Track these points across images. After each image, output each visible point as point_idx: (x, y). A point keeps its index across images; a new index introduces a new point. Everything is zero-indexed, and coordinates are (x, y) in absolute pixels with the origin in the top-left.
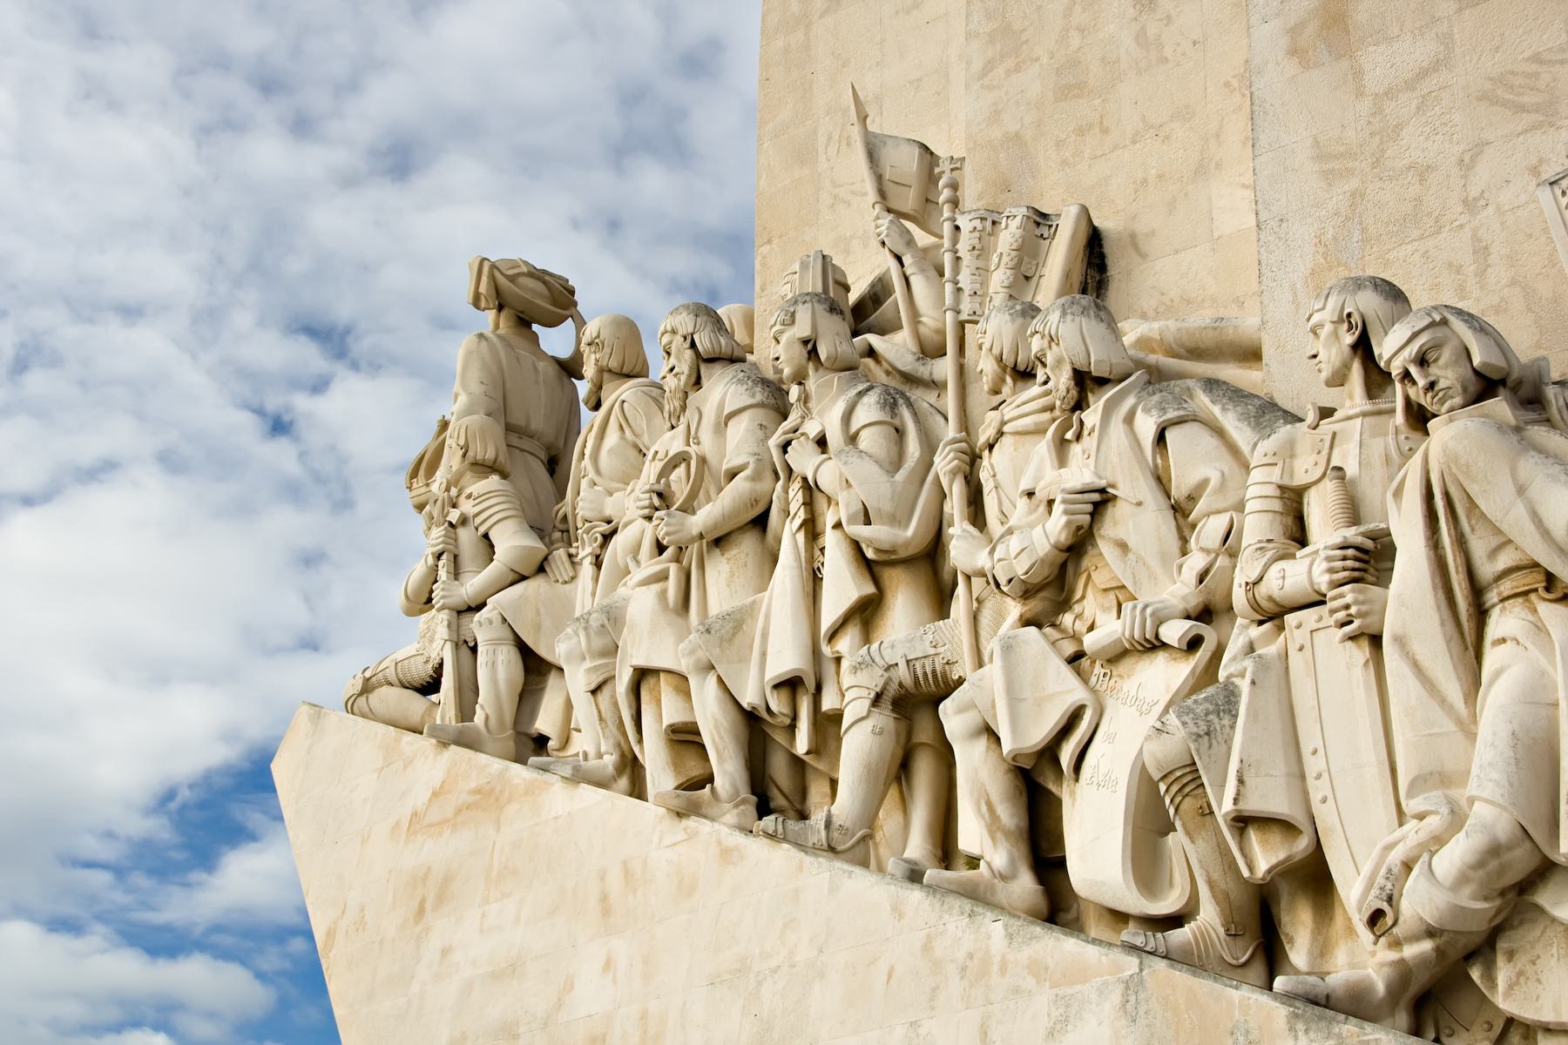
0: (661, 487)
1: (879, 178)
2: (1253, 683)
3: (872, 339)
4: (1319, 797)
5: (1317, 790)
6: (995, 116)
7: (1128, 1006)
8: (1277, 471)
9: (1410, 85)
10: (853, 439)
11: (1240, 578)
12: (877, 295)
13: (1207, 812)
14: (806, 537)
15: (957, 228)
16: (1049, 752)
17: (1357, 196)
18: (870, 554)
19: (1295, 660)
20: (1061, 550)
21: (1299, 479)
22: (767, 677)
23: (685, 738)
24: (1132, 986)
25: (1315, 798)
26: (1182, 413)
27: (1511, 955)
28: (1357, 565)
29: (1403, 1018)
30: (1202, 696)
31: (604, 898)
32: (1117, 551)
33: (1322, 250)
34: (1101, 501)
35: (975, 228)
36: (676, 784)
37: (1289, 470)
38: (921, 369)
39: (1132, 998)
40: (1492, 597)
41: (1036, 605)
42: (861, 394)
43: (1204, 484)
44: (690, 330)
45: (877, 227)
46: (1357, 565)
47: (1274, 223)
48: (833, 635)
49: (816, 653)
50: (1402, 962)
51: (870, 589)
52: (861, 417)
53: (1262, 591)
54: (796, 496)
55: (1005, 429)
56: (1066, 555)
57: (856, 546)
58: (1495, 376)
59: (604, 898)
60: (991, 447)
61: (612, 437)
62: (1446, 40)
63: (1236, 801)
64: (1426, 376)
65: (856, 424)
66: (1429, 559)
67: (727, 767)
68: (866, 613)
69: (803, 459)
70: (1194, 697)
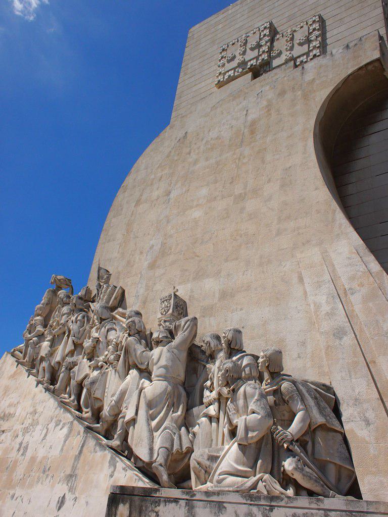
1: (99, 275)
29: (103, 433)
51: (73, 348)
52: (79, 318)
57: (73, 341)
68: (72, 353)
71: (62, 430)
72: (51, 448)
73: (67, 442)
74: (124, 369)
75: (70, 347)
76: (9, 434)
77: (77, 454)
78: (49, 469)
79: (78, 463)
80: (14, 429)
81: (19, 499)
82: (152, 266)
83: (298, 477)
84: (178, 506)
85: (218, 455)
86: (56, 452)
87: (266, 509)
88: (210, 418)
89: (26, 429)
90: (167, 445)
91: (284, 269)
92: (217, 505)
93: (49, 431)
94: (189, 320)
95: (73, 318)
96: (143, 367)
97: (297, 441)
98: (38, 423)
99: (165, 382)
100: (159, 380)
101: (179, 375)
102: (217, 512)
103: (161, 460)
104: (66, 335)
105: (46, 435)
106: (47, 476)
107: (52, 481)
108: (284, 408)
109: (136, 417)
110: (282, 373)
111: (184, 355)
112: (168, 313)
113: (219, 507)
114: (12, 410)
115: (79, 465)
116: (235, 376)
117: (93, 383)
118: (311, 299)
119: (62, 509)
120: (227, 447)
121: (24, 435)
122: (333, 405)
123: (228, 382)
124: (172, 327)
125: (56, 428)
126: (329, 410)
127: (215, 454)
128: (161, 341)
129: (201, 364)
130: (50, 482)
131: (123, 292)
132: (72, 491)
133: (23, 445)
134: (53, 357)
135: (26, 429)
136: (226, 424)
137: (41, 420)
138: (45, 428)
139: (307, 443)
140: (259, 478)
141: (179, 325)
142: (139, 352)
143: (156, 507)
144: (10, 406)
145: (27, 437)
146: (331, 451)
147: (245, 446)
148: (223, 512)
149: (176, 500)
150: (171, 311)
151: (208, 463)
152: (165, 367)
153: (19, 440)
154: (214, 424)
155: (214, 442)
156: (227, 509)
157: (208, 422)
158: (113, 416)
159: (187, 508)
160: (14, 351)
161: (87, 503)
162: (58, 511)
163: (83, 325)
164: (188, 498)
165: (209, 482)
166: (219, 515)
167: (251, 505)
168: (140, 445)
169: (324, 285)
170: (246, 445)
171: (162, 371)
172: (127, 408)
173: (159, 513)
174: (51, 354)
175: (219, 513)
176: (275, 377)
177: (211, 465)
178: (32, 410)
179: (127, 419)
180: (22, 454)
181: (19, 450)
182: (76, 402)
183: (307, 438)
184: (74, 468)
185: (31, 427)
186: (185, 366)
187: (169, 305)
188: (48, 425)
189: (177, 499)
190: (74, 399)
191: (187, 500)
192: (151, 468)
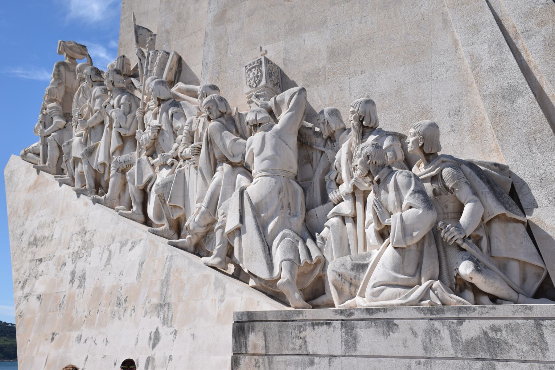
14: (109, 129)
16: (146, 186)
20: (152, 140)
29: (192, 249)
32: (162, 141)
37: (191, 127)
43: (179, 127)
47: (205, 64)
48: (113, 154)
50: (190, 238)
51: (121, 143)
52: (122, 101)
54: (107, 118)
71: (134, 250)
72: (121, 274)
73: (144, 265)
75: (115, 143)
76: (51, 262)
77: (163, 278)
78: (126, 301)
79: (167, 289)
80: (57, 254)
81: (89, 341)
83: (479, 281)
84: (332, 328)
85: (366, 262)
86: (131, 279)
87: (453, 323)
88: (343, 219)
89: (75, 254)
90: (291, 257)
91: (422, 10)
92: (385, 323)
93: (112, 254)
94: (295, 93)
95: (114, 102)
96: (237, 160)
97: (469, 238)
98: (92, 245)
100: (265, 176)
101: (291, 167)
102: (386, 331)
103: (285, 276)
104: (107, 125)
105: (109, 259)
106: (125, 309)
107: (133, 315)
108: (447, 199)
109: (241, 225)
110: (439, 154)
111: (293, 141)
112: (261, 85)
113: (388, 325)
114: (46, 232)
115: (169, 292)
116: (379, 162)
117: (166, 185)
118: (462, 52)
119: (157, 347)
120: (375, 253)
121: (74, 261)
122: (509, 189)
123: (369, 172)
124: (271, 103)
125: (124, 248)
126: (507, 196)
127: (361, 262)
128: (260, 124)
130: (131, 316)
131: (180, 59)
132: (167, 323)
133: (77, 275)
135: (75, 254)
136: (369, 224)
137: (96, 240)
138: (105, 251)
139: (481, 238)
140: (427, 286)
141: (282, 101)
143: (300, 332)
144: (40, 227)
145: (81, 265)
146: (513, 246)
147: (402, 249)
148: (394, 330)
149: (328, 322)
150: (263, 82)
151: (353, 274)
153: (69, 268)
154: (349, 225)
155: (352, 248)
156: (400, 326)
158: (204, 226)
159: (344, 330)
160: (26, 153)
161: (193, 335)
162: (152, 349)
164: (344, 318)
165: (359, 295)
166: (390, 335)
167: (431, 319)
168: (253, 259)
169: (484, 28)
170: (404, 248)
172: (225, 215)
173: (307, 339)
174: (90, 152)
175: (388, 332)
176: (431, 159)
177: (358, 276)
178: (78, 229)
179: (229, 228)
180: (78, 286)
181: (72, 281)
183: (482, 233)
184: (163, 296)
185: (83, 251)
186: (297, 154)
187: (259, 74)
188: (109, 246)
189: (328, 320)
191: (342, 320)
192: (276, 287)
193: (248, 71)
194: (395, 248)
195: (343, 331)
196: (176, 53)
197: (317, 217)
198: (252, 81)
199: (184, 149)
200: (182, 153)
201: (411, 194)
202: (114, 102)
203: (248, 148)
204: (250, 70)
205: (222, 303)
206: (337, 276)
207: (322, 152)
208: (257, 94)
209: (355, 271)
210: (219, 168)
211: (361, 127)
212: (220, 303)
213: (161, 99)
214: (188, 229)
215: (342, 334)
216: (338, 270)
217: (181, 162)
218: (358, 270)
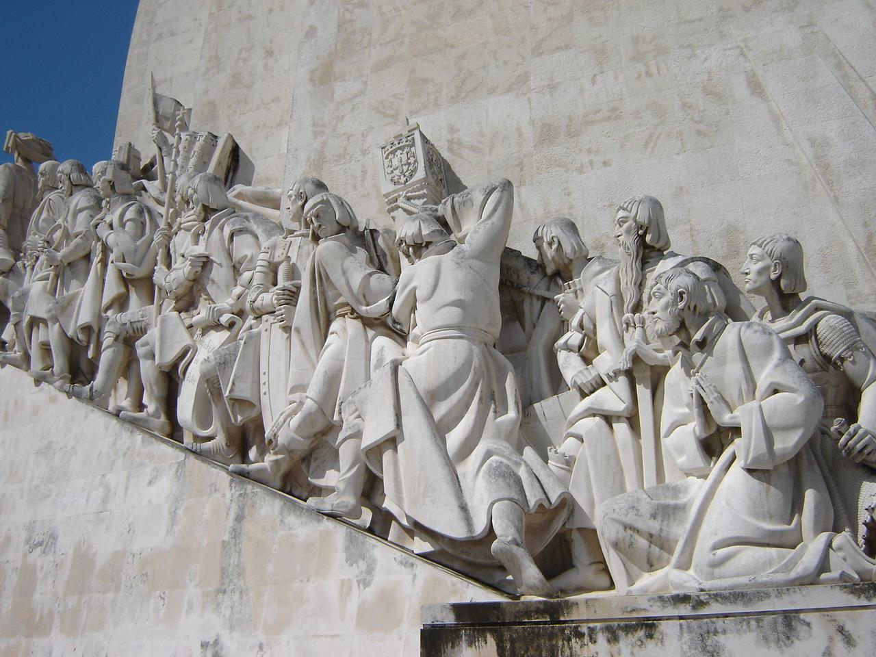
0: (48, 239)
1: (157, 113)
2: (245, 343)
3: (145, 182)
4: (264, 391)
5: (263, 389)
6: (206, 92)
7: (178, 473)
8: (268, 255)
9: (350, 100)
10: (123, 225)
11: (249, 299)
12: (152, 164)
13: (220, 394)
15: (181, 138)
16: (175, 366)
17: (324, 143)
18: (125, 275)
19: (264, 336)
21: (276, 259)
22: (78, 325)
23: (46, 348)
24: (181, 465)
25: (262, 391)
26: (241, 227)
27: (316, 459)
28: (288, 298)
29: (278, 483)
30: (226, 347)
31: (6, 414)
33: (308, 164)
34: (205, 263)
35: (187, 140)
36: (41, 367)
38: (161, 197)
39: (180, 470)
40: (332, 316)
41: (181, 304)
42: (130, 206)
43: (247, 256)
44: (69, 172)
45: (153, 134)
46: (288, 298)
49: (100, 316)
51: (123, 290)
53: (258, 303)
54: (99, 246)
55: (182, 226)
56: (192, 283)
57: (120, 272)
58: (345, 225)
59: (6, 414)
60: (176, 234)
61: (44, 215)
62: (365, 83)
63: (230, 393)
64: (318, 221)
65: (125, 220)
66: (310, 297)
67: (59, 362)
68: (121, 303)
69: (103, 232)
70: (223, 347)
73: (180, 512)
74: (315, 320)
75: (112, 288)
82: (324, 77)
88: (609, 419)
95: (114, 217)
99: (463, 344)
104: (96, 260)
105: (105, 501)
112: (414, 179)
129: (531, 295)
131: (235, 151)
134: (71, 316)
142: (356, 279)
150: (421, 174)
152: (458, 304)
157: (603, 423)
163: (143, 234)
171: (453, 314)
174: (65, 307)
179: (368, 439)
182: (163, 418)
187: (412, 160)
190: (156, 411)
191: (681, 618)
193: (388, 155)
194: (750, 471)
195: (683, 641)
196: (230, 136)
197: (546, 420)
198: (397, 172)
199: (258, 295)
200: (254, 302)
201: (777, 366)
202: (114, 217)
203: (405, 287)
204: (393, 153)
205: (367, 589)
206: (621, 528)
207: (544, 300)
208: (410, 194)
209: (659, 518)
210: (335, 326)
211: (642, 248)
212: (361, 586)
213: (211, 207)
214: (274, 444)
215: (682, 648)
216: (624, 519)
217: (250, 320)
218: (667, 516)
